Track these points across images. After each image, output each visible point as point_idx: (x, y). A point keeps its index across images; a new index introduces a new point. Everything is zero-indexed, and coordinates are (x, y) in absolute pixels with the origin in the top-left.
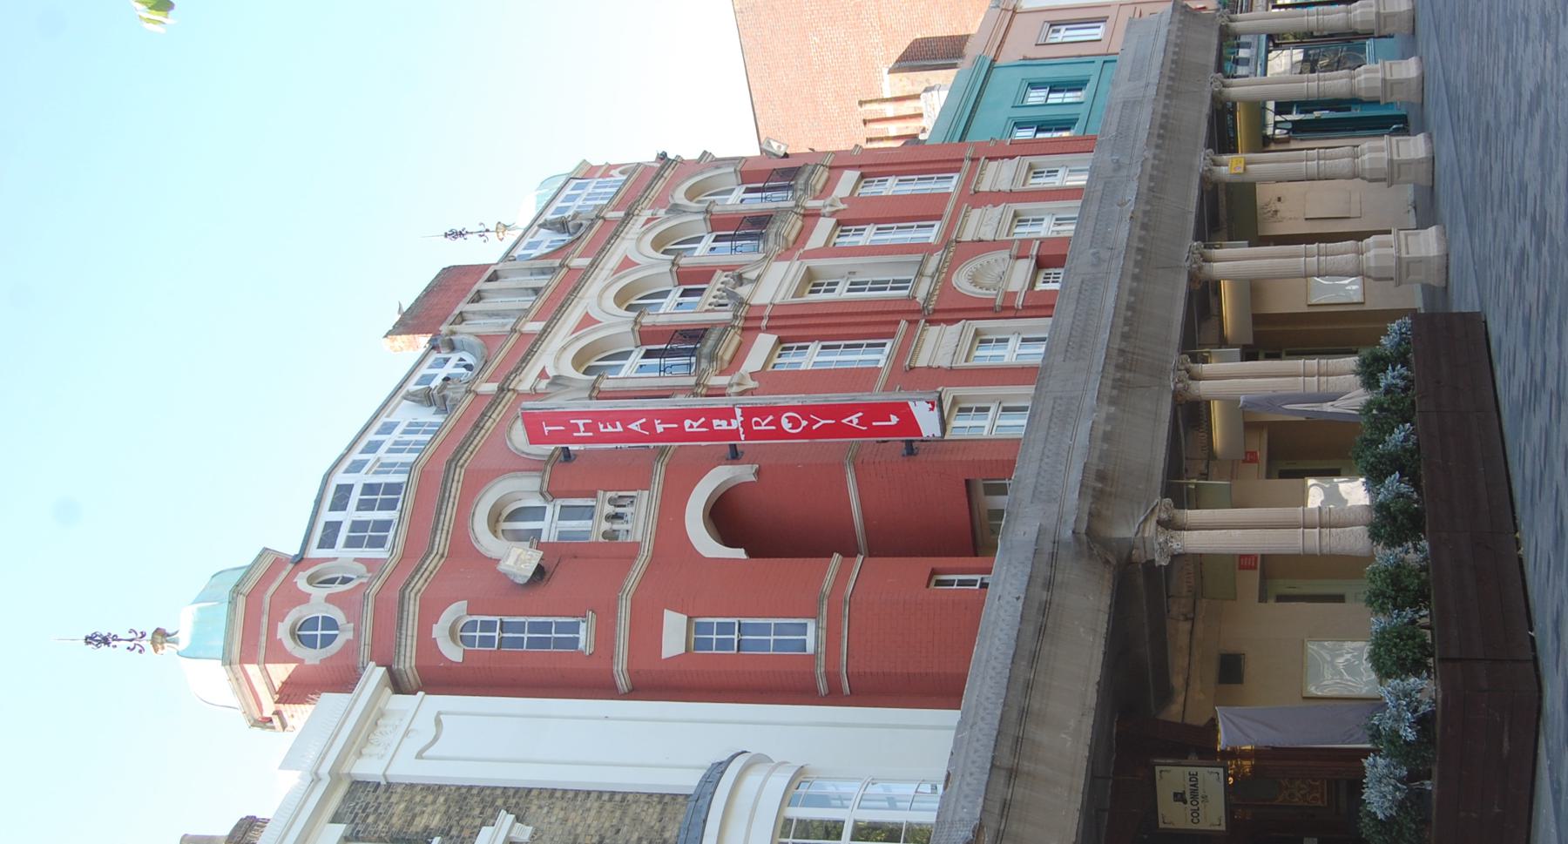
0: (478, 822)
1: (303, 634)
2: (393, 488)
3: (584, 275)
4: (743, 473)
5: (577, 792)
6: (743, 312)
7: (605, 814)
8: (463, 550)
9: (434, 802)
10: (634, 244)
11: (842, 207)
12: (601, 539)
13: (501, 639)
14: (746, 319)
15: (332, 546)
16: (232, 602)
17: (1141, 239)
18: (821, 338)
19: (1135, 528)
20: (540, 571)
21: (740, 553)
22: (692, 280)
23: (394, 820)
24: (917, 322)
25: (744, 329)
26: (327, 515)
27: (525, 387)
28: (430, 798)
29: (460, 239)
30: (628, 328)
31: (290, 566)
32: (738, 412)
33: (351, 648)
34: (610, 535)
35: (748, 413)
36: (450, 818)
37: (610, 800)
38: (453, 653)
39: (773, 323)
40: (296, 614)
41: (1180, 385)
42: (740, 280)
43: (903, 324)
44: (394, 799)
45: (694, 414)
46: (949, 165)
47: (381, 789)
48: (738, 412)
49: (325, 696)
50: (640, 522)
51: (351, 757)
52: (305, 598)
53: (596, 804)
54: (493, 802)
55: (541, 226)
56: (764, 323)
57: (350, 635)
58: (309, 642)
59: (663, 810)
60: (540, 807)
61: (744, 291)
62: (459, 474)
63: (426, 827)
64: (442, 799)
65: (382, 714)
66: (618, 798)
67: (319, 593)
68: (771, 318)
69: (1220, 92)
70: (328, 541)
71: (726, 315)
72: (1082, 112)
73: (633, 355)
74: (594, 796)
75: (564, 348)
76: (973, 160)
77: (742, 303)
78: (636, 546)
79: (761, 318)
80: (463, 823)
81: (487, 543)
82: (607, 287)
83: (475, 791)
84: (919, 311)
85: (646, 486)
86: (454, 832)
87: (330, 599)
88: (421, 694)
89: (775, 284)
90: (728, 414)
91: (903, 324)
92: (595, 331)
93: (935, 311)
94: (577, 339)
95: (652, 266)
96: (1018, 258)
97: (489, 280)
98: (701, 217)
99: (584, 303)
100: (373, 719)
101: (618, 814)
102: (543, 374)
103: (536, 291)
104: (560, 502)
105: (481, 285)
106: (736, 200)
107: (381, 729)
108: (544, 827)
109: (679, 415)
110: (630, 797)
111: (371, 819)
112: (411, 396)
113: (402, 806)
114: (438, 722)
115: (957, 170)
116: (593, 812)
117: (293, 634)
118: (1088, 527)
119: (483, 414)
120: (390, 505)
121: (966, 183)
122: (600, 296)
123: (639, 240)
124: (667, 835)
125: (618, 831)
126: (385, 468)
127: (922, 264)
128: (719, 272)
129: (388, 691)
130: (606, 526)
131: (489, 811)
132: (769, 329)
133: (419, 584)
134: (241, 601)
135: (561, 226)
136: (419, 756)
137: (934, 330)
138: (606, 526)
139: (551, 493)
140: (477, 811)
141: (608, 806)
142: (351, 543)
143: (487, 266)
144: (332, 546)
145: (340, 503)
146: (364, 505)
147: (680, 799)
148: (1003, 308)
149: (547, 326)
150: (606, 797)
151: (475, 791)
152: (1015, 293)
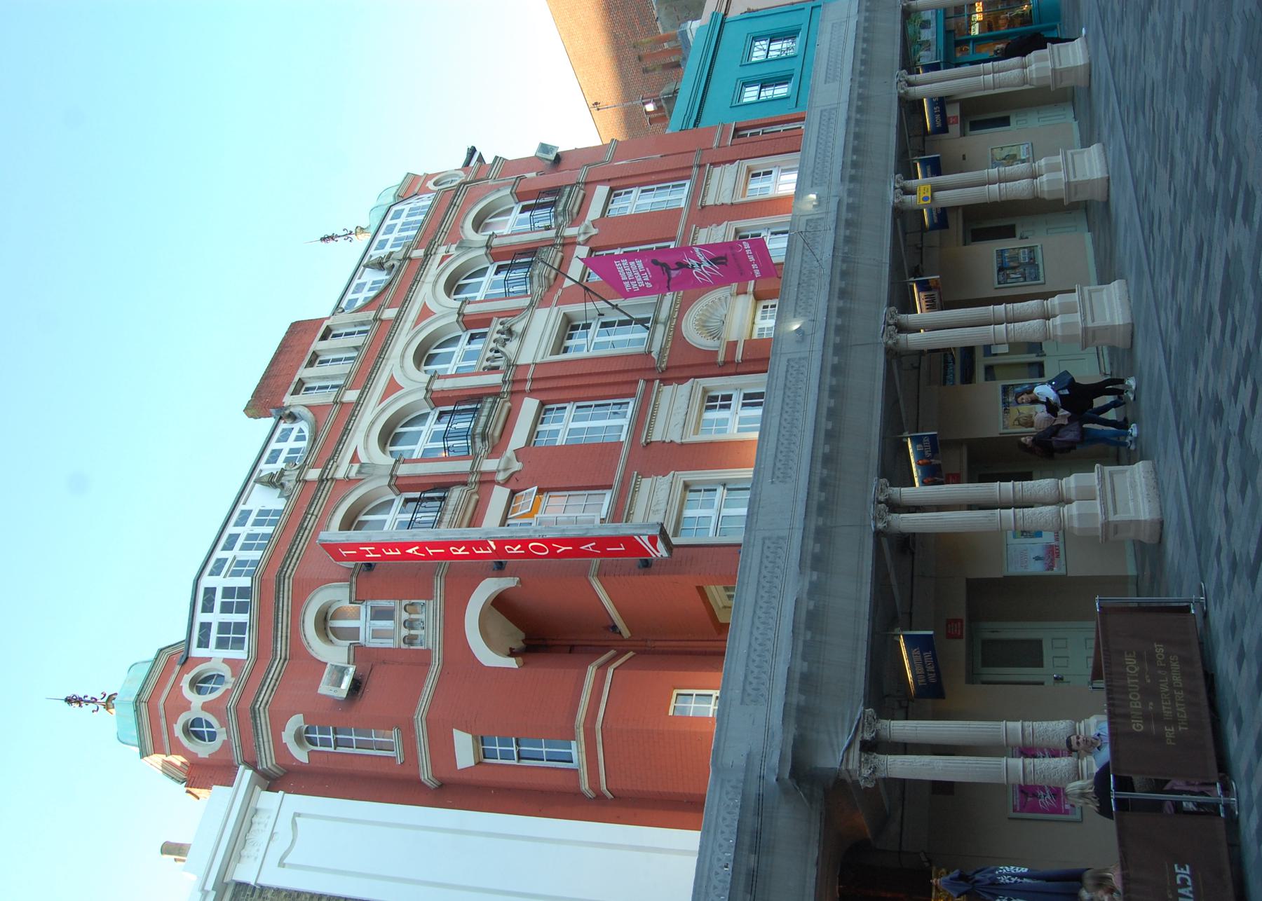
1: (194, 730)
2: (244, 592)
3: (358, 403)
4: (507, 583)
6: (509, 377)
8: (298, 651)
10: (430, 292)
11: (594, 231)
12: (404, 646)
13: (336, 740)
14: (514, 382)
15: (207, 646)
16: (137, 710)
17: (841, 312)
18: (575, 400)
19: (836, 753)
20: (356, 686)
21: (512, 663)
22: (474, 324)
24: (653, 381)
25: (512, 393)
26: (201, 617)
27: (340, 474)
29: (331, 242)
30: (421, 395)
31: (178, 668)
32: (492, 544)
33: (226, 745)
34: (410, 640)
35: (500, 543)
38: (301, 755)
39: (536, 386)
40: (184, 718)
41: (880, 525)
42: (510, 332)
43: (641, 383)
45: (458, 544)
46: (680, 174)
47: (257, 893)
48: (492, 544)
49: (214, 787)
50: (430, 636)
51: (232, 863)
52: (186, 706)
55: (366, 266)
56: (528, 386)
57: (225, 737)
58: (200, 736)
61: (512, 347)
62: (288, 585)
65: (256, 811)
67: (196, 700)
68: (533, 380)
69: (906, 93)
70: (203, 643)
71: (496, 379)
72: (796, 66)
73: (396, 503)
75: (373, 423)
76: (701, 166)
77: (510, 365)
78: (428, 652)
79: (526, 381)
81: (318, 647)
82: (408, 344)
84: (654, 369)
85: (430, 597)
87: (206, 707)
88: (281, 793)
89: (534, 346)
90: (484, 544)
91: (641, 383)
92: (396, 400)
93: (667, 368)
94: (383, 410)
95: (443, 316)
96: (738, 294)
97: (324, 338)
98: (483, 251)
99: (388, 369)
100: (247, 817)
102: (355, 458)
103: (356, 348)
104: (369, 603)
105: (318, 345)
106: (513, 226)
107: (255, 827)
109: (446, 545)
112: (258, 481)
114: (294, 823)
115: (688, 178)
117: (186, 731)
118: (793, 767)
119: (307, 513)
120: (242, 609)
121: (694, 196)
122: (403, 356)
123: (436, 282)
126: (240, 567)
127: (658, 306)
128: (495, 319)
129: (258, 788)
130: (405, 632)
132: (532, 393)
133: (264, 696)
134: (144, 707)
135: (379, 265)
136: (281, 864)
137: (667, 390)
138: (405, 632)
139: (358, 598)
142: (222, 644)
143: (321, 321)
144: (207, 646)
145: (208, 608)
146: (226, 608)
148: (725, 363)
149: (362, 393)
152: (735, 343)
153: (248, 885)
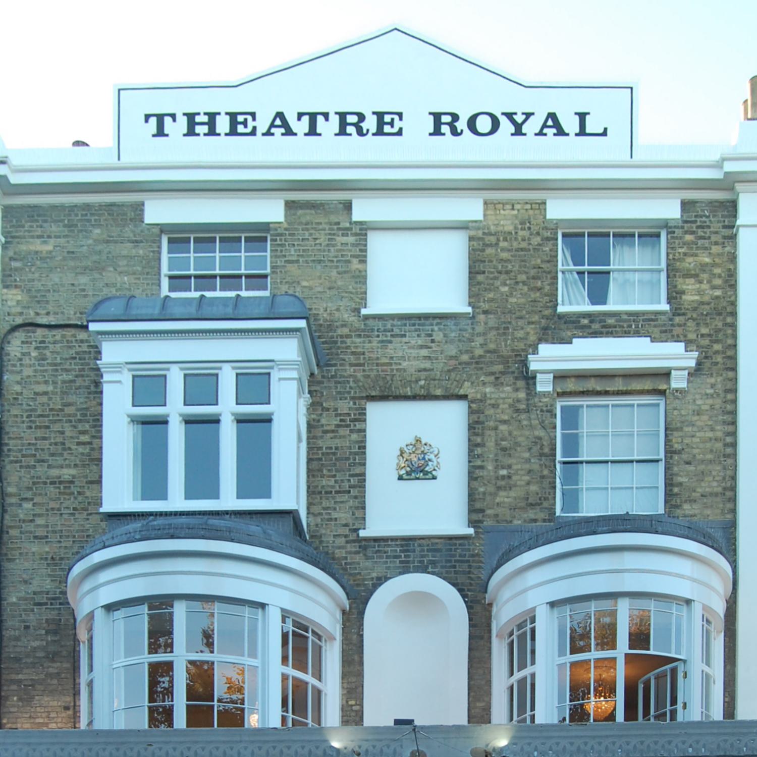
0: (692, 336)
5: (734, 413)
7: (708, 445)
9: (714, 288)
23: (690, 259)
28: (718, 282)
36: (695, 309)
37: (726, 445)
44: (715, 249)
53: (719, 434)
54: (717, 341)
59: (716, 495)
60: (713, 386)
63: (683, 292)
64: (718, 293)
66: (729, 450)
74: (730, 428)
80: (690, 324)
83: (729, 320)
86: (677, 320)
101: (709, 456)
108: (689, 397)
110: (730, 461)
111: (689, 238)
113: (707, 260)
116: (710, 434)
124: (686, 506)
125: (688, 463)
131: (706, 342)
140: (704, 331)
141: (719, 445)
147: (729, 506)
150: (729, 440)
151: (729, 320)
153: (735, 216)
